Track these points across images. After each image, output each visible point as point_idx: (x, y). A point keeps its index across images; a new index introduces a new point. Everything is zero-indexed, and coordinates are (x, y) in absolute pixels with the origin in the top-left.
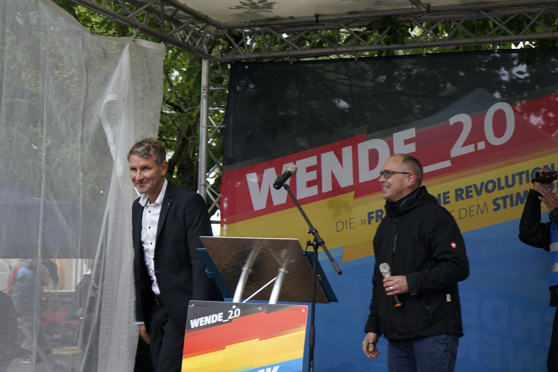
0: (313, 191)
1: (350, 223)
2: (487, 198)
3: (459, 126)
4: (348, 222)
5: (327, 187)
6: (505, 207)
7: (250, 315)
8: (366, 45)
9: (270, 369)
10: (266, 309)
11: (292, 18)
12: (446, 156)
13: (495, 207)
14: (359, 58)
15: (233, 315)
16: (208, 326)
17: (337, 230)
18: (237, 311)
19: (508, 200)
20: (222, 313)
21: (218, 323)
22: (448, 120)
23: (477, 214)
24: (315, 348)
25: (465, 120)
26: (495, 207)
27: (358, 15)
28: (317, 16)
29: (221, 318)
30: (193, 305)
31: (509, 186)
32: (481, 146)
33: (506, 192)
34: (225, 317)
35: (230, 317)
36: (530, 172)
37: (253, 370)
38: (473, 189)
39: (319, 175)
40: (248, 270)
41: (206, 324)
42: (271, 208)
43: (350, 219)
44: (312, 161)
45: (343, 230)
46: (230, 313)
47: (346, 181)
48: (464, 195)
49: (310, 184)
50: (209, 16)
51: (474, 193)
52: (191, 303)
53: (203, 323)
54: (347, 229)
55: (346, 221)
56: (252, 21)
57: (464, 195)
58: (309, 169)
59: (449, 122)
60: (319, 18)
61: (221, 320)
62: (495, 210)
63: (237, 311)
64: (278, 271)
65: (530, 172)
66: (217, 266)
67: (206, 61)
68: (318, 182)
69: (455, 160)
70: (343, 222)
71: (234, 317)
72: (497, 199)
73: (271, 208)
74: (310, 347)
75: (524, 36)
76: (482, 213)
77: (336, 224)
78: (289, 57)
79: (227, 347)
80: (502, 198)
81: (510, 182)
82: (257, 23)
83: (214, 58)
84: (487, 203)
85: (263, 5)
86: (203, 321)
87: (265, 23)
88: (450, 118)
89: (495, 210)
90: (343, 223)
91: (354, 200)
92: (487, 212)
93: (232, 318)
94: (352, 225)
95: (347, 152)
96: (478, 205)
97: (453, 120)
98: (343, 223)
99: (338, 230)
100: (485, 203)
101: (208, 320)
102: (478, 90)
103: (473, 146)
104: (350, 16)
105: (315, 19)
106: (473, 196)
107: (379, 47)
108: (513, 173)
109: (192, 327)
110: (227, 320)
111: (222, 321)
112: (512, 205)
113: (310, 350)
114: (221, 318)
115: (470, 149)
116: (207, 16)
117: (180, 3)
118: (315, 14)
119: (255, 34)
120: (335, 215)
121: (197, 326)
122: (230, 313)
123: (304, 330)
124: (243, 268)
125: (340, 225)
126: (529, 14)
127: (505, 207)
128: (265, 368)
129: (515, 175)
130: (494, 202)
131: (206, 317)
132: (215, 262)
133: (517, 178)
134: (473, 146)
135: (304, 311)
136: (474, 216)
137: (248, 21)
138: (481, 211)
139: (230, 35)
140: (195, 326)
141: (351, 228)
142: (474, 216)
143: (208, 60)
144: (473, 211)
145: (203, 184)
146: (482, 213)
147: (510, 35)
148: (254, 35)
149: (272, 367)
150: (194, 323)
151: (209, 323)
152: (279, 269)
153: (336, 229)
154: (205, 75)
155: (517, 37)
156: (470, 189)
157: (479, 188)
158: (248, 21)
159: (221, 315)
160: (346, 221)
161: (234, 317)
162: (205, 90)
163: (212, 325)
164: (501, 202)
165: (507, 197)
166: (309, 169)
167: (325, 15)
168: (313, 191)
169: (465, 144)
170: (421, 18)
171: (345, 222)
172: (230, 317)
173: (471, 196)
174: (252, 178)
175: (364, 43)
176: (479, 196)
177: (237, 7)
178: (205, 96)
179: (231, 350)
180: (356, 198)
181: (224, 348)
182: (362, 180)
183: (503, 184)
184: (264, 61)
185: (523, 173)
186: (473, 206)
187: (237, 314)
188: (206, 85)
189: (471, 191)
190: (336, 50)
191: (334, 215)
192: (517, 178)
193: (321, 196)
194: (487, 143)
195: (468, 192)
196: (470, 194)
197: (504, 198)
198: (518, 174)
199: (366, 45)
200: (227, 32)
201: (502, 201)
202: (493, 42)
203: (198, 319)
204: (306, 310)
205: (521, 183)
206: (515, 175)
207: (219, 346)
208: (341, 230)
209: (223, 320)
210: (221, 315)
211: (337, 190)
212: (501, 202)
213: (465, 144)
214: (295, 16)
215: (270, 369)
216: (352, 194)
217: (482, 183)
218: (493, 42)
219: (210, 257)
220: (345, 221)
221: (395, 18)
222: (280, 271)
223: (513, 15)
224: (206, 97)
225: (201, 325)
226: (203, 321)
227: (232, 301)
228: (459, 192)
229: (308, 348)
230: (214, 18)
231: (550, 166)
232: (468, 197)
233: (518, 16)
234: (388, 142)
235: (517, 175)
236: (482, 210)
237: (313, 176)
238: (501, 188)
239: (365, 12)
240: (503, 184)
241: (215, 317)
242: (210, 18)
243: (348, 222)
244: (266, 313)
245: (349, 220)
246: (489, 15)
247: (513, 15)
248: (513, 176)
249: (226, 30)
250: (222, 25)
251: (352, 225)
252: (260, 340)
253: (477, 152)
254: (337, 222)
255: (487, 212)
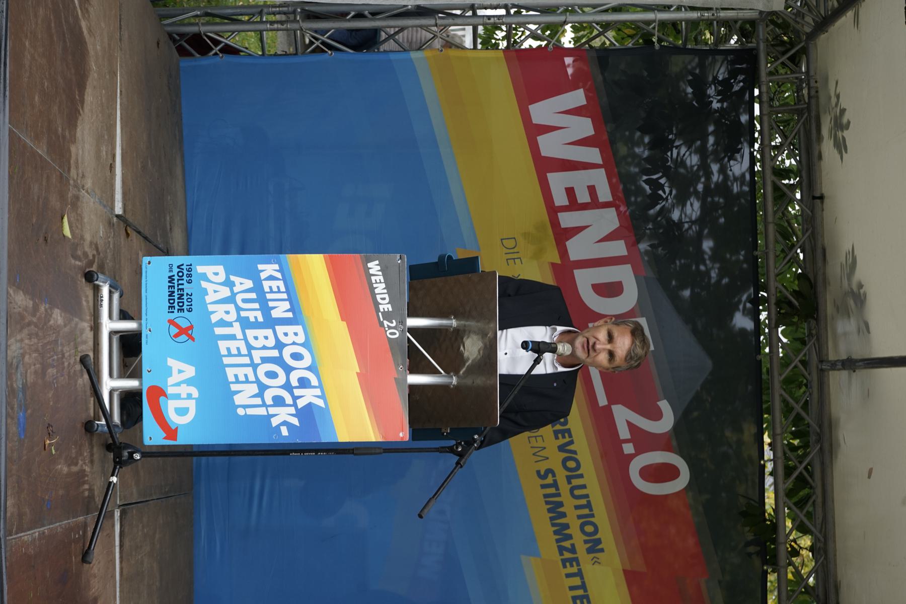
0: (561, 199)
1: (514, 259)
2: (555, 460)
3: (656, 415)
4: (515, 256)
5: (567, 220)
6: (543, 486)
7: (390, 354)
8: (777, 269)
9: (320, 394)
10: (400, 377)
11: (820, 157)
12: (613, 399)
13: (542, 473)
14: (757, 256)
15: (390, 328)
16: (372, 289)
17: (503, 239)
18: (394, 334)
19: (552, 491)
20: (390, 309)
21: (377, 304)
22: (665, 399)
23: (532, 447)
24: (351, 456)
25: (666, 423)
26: (542, 473)
27: (820, 263)
28: (822, 198)
29: (384, 309)
30: (399, 262)
31: (572, 490)
32: (628, 449)
33: (564, 488)
34: (387, 316)
35: (386, 323)
36: (591, 519)
37: (317, 367)
38: (567, 439)
39: (584, 207)
40: (451, 326)
41: (375, 286)
42: (534, 131)
43: (520, 258)
44: (605, 194)
45: (505, 248)
46: (392, 323)
47: (577, 249)
48: (558, 427)
49: (570, 192)
50: (826, 34)
51: (561, 441)
52: (402, 258)
53: (376, 280)
54: (506, 254)
55: (518, 252)
56: (817, 92)
57: (558, 427)
58: (592, 190)
59: (663, 400)
60: (818, 201)
61: (382, 310)
62: (538, 472)
63: (394, 334)
64: (452, 374)
65: (591, 519)
66: (456, 277)
67: (757, 14)
68: (574, 205)
69: (607, 410)
70: (515, 248)
71: (387, 329)
72: (554, 475)
73: (534, 131)
74: (353, 450)
75: (782, 503)
76: (534, 454)
77: (513, 237)
78: (762, 147)
79: (343, 325)
80: (555, 481)
81: (577, 492)
82: (813, 101)
83: (762, 23)
84: (547, 461)
85: (839, 137)
86: (378, 281)
87: (813, 114)
88: (667, 401)
89: (538, 472)
90: (514, 248)
91: (549, 262)
92: (536, 462)
93: (386, 326)
94: (511, 262)
95: (619, 248)
96: (545, 448)
97: (664, 405)
98: (514, 248)
99: (504, 241)
100: (547, 458)
101: (380, 288)
102: (709, 364)
103: (628, 436)
104: (819, 252)
105: (818, 194)
106: (557, 441)
107: (773, 290)
108: (590, 496)
109: (370, 265)
110: (382, 320)
111: (380, 311)
112: (546, 496)
113: (349, 450)
114: (384, 309)
115: (624, 433)
116: (827, 32)
117: (848, 12)
118: (825, 195)
119: (798, 83)
120: (526, 235)
121: (371, 271)
122: (392, 323)
123: (376, 438)
124: (454, 318)
125: (511, 243)
126: (814, 502)
127: (543, 486)
128: (320, 386)
129: (588, 499)
130: (549, 471)
131: (383, 285)
132: (461, 277)
133: (583, 502)
134: (628, 436)
135: (401, 435)
136: (530, 443)
137: (818, 85)
138: (536, 453)
139: (797, 51)
140: (371, 268)
141: (507, 260)
142: (530, 443)
143: (758, 17)
144: (537, 441)
145: (567, 20)
146: (534, 454)
147: (784, 483)
148: (797, 81)
149: (323, 397)
150: (374, 267)
151: (377, 291)
152: (455, 376)
153: (504, 238)
154: (737, 14)
155: (782, 494)
156: (566, 435)
157: (568, 448)
158: (818, 85)
159: (388, 308)
160: (518, 252)
161: (387, 329)
162: (713, 15)
163: (374, 295)
164: (549, 480)
165: (557, 489)
166: (592, 190)
167: (823, 210)
168: (561, 199)
169: (631, 425)
170: (814, 350)
171: (515, 250)
172: (386, 323)
173: (557, 438)
174: (577, 98)
175: (780, 265)
176: (557, 448)
177: (839, 94)
178: (704, 16)
179: (340, 331)
180: (551, 266)
181: (343, 319)
182: (578, 273)
183: (575, 482)
184: (755, 104)
185: (591, 510)
186: (543, 441)
187: (391, 334)
188: (720, 16)
189: (564, 437)
190: (770, 223)
191: (525, 233)
192: (583, 502)
193: (553, 211)
194: (631, 457)
195: (563, 432)
196: (560, 436)
197: (555, 485)
198: (589, 502)
199: (777, 269)
200: (803, 46)
201: (552, 482)
202: (776, 459)
203: (380, 273)
204: (402, 438)
205: (577, 507)
206: (588, 499)
207: (345, 314)
208: (504, 244)
209: (382, 312)
210: (388, 308)
211: (562, 235)
212: (549, 480)
213: (631, 425)
214: (822, 163)
215: (320, 394)
216: (558, 261)
217: (575, 452)
218: (776, 459)
219: (468, 273)
220: (517, 251)
221: (813, 318)
222: (453, 379)
223: (813, 481)
224: (703, 17)
225: (373, 278)
226: (379, 282)
227: (409, 316)
228: (562, 420)
229: (352, 447)
230: (823, 37)
231: (600, 547)
232: (556, 433)
233: (811, 487)
234: (632, 310)
235: (587, 501)
236: (537, 454)
237: (583, 197)
238: (569, 479)
239: (824, 274)
240: (575, 482)
241: (384, 299)
242: (824, 34)
243: (515, 256)
244: (395, 378)
245: (519, 257)
246: (816, 453)
247: (813, 481)
248: (587, 496)
249: (805, 46)
250: (812, 42)
251: (511, 262)
252: (357, 373)
253: (618, 443)
254: (515, 238)
255: (536, 462)
